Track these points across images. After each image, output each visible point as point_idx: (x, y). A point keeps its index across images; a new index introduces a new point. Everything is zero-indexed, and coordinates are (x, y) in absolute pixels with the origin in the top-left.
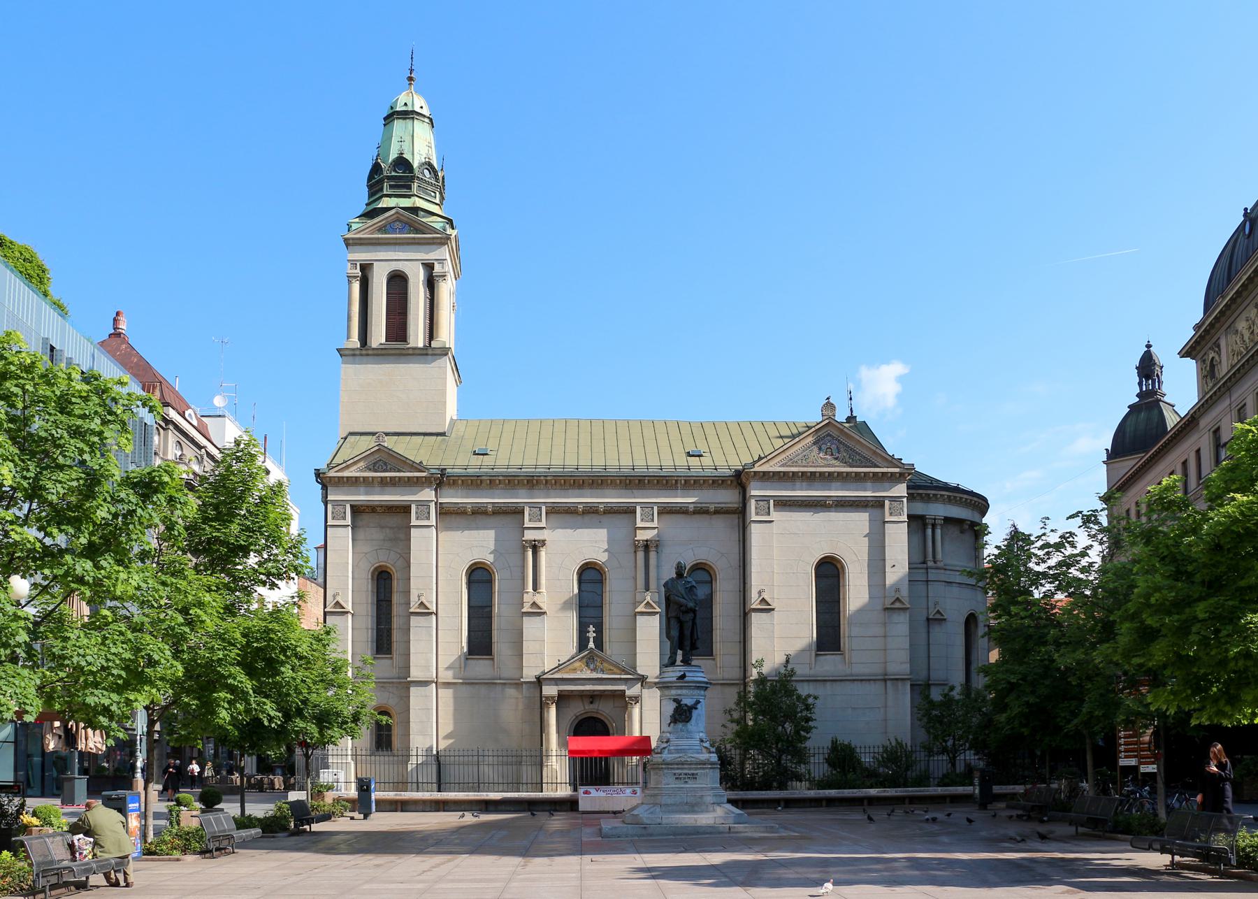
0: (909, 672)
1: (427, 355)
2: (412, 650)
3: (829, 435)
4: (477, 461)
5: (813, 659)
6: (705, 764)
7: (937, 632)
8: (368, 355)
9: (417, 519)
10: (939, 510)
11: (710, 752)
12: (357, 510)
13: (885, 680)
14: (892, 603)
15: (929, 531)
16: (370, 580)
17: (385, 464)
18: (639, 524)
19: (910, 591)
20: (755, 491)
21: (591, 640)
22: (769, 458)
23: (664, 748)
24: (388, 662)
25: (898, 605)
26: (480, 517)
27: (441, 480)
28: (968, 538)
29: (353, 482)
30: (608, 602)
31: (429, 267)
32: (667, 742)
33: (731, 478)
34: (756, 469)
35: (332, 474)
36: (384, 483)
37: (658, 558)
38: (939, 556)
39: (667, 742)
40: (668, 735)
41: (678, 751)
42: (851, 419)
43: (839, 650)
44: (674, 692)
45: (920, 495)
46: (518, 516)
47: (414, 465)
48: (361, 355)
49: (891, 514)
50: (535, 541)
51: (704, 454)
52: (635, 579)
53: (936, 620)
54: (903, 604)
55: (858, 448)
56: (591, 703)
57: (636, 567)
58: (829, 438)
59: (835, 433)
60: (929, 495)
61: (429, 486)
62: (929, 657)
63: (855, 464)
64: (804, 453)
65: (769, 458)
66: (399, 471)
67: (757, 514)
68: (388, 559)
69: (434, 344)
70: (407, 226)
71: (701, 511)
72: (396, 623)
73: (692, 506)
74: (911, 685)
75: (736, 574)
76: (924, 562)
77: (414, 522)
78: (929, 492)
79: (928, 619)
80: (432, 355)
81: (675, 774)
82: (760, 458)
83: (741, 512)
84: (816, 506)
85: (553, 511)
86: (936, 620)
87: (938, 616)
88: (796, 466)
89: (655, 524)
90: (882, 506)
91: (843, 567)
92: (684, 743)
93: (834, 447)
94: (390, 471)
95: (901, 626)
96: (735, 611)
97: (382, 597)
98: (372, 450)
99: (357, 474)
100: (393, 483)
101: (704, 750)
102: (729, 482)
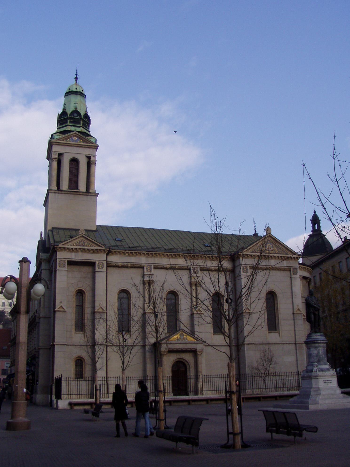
1: (88, 195)
8: (61, 193)
12: (71, 263)
17: (84, 242)
36: (84, 251)
48: (58, 193)
49: (294, 274)
63: (279, 253)
67: (243, 272)
93: (271, 246)
99: (72, 247)
100: (89, 251)
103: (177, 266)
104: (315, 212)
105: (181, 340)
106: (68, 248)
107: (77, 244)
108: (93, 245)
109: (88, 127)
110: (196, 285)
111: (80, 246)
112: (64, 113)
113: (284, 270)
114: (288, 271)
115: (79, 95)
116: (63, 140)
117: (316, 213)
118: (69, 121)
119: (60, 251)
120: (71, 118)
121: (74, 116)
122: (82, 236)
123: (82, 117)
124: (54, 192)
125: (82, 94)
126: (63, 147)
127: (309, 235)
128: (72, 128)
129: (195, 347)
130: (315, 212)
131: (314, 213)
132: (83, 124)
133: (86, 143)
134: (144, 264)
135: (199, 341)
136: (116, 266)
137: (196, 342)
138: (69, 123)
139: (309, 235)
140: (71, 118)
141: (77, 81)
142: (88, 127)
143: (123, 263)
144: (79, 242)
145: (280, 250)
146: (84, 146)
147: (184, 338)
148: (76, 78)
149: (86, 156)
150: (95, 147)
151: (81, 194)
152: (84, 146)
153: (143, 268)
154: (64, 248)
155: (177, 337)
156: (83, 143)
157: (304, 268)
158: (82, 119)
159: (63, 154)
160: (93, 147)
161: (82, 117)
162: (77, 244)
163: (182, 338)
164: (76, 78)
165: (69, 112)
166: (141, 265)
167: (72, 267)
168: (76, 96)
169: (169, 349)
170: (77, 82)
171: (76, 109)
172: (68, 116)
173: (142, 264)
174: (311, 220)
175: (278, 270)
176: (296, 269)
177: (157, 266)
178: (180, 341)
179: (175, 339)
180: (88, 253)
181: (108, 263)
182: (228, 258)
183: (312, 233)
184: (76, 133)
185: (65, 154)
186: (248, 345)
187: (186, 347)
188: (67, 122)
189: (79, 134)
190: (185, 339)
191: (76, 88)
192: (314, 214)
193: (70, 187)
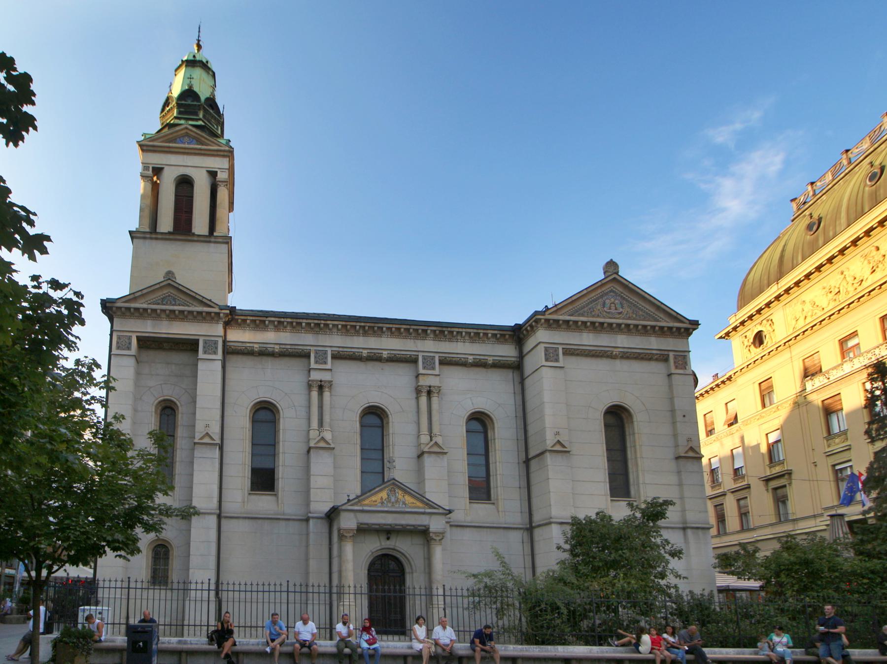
2: (195, 481)
9: (205, 352)
16: (153, 413)
17: (174, 299)
26: (265, 358)
33: (509, 333)
36: (173, 316)
46: (304, 360)
50: (321, 381)
52: (418, 424)
56: (388, 539)
68: (170, 392)
70: (195, 141)
71: (480, 364)
73: (471, 357)
77: (201, 354)
83: (517, 367)
85: (338, 356)
89: (437, 372)
98: (162, 284)
99: (145, 306)
105: (390, 505)
106: (137, 309)
108: (194, 304)
109: (215, 127)
110: (429, 393)
122: (169, 284)
129: (425, 523)
134: (308, 348)
135: (435, 508)
142: (215, 127)
143: (262, 345)
144: (162, 299)
146: (203, 152)
147: (397, 501)
149: (207, 171)
150: (226, 154)
152: (203, 152)
153: (307, 356)
154: (128, 309)
158: (201, 105)
160: (222, 153)
162: (160, 301)
163: (393, 499)
167: (151, 355)
169: (361, 524)
177: (339, 352)
178: (387, 506)
179: (376, 501)
180: (182, 320)
185: (166, 169)
187: (403, 522)
190: (401, 503)
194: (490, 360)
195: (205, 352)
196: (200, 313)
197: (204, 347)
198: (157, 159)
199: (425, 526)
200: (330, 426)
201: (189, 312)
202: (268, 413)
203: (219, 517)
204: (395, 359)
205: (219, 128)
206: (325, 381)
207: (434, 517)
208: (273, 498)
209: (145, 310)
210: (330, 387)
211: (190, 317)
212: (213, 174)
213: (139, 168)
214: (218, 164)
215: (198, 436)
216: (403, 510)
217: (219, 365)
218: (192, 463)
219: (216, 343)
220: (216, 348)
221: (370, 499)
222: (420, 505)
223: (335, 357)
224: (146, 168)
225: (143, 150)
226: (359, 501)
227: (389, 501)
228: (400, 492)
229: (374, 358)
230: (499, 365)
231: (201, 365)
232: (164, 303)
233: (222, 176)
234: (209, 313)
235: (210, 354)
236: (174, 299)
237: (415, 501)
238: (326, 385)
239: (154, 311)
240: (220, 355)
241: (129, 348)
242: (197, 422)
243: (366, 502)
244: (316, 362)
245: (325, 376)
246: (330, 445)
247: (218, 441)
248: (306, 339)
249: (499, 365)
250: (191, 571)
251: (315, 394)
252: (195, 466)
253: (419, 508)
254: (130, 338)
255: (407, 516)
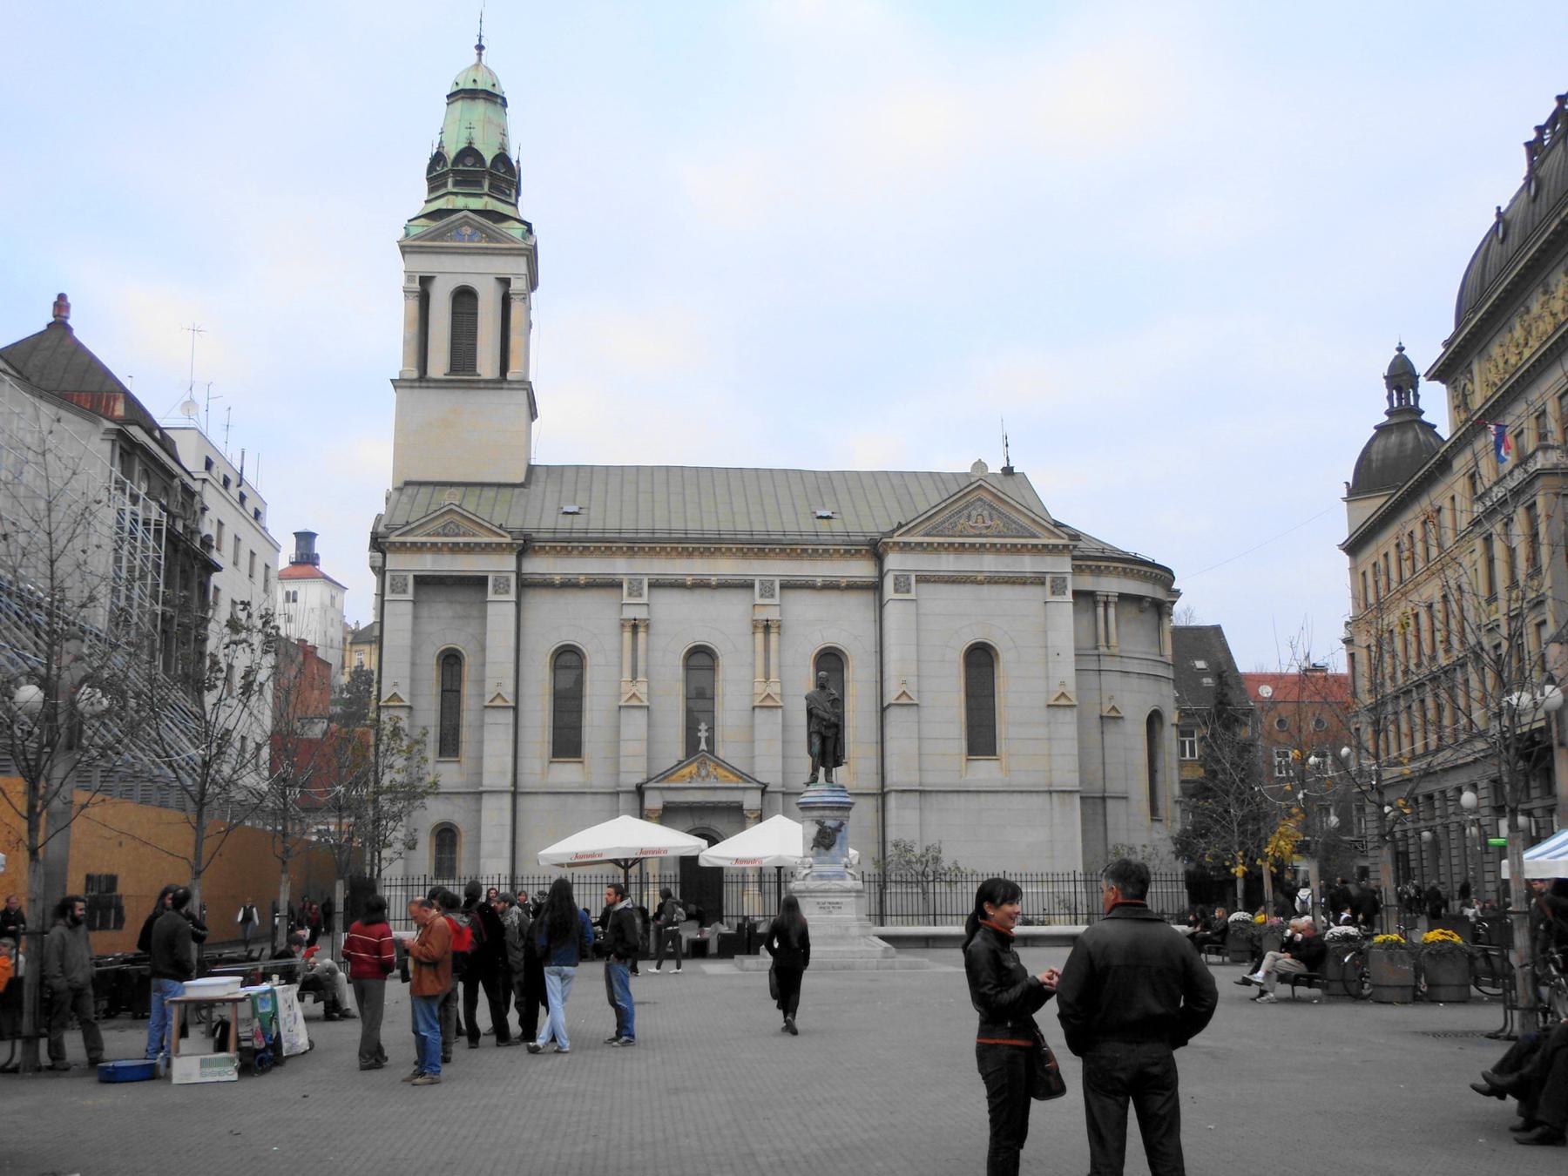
0: (1078, 783)
1: (502, 389)
3: (980, 499)
4: (565, 523)
5: (964, 764)
6: (850, 892)
7: (1113, 736)
8: (428, 387)
9: (496, 592)
10: (1111, 585)
11: (855, 879)
12: (424, 582)
13: (1050, 792)
14: (1057, 699)
15: (1101, 610)
17: (458, 526)
18: (759, 601)
19: (1079, 687)
20: (893, 561)
21: (703, 740)
22: (910, 525)
23: (807, 875)
24: (454, 766)
25: (1063, 702)
27: (525, 546)
28: (1150, 617)
29: (418, 548)
30: (720, 693)
31: (505, 282)
32: (810, 867)
34: (896, 539)
35: (393, 538)
36: (455, 549)
37: (780, 640)
38: (1113, 641)
39: (810, 867)
40: (811, 859)
41: (821, 877)
42: (1008, 471)
43: (995, 755)
44: (816, 813)
45: (1089, 567)
46: (618, 591)
47: (494, 528)
48: (420, 387)
49: (1053, 593)
51: (834, 516)
52: (753, 665)
53: (1110, 719)
54: (1070, 699)
55: (1014, 515)
57: (754, 652)
58: (979, 503)
59: (988, 498)
60: (1100, 567)
61: (511, 553)
62: (1104, 763)
64: (951, 521)
65: (910, 525)
66: (474, 535)
67: (896, 591)
68: (456, 638)
69: (510, 376)
71: (831, 586)
72: (468, 717)
74: (1081, 798)
75: (873, 660)
76: (1096, 648)
77: (491, 596)
78: (1100, 563)
79: (1102, 717)
80: (509, 389)
81: (818, 903)
82: (900, 526)
83: (876, 587)
84: (965, 582)
86: (1110, 719)
87: (1113, 714)
88: (941, 536)
90: (1043, 583)
91: (997, 655)
92: (826, 869)
93: (985, 513)
94: (464, 535)
95: (1067, 725)
96: (871, 706)
97: (448, 687)
99: (424, 539)
100: (469, 549)
101: (849, 877)
102: (864, 552)
103: (713, 578)
104: (1401, 349)
105: (699, 780)
106: (414, 544)
107: (440, 530)
111: (446, 535)
112: (438, 158)
113: (1024, 583)
114: (1036, 584)
115: (481, 101)
116: (433, 239)
117: (1404, 352)
118: (450, 181)
119: (391, 551)
120: (456, 173)
121: (465, 165)
122: (451, 510)
123: (488, 162)
124: (408, 384)
125: (494, 98)
126: (433, 258)
127: (1376, 427)
128: (460, 202)
130: (1401, 349)
131: (1397, 353)
132: (491, 186)
133: (498, 242)
136: (546, 584)
137: (742, 785)
138: (450, 188)
139: (1376, 427)
140: (456, 173)
141: (480, 55)
145: (1014, 526)
148: (480, 48)
151: (482, 385)
153: (620, 585)
154: (404, 544)
155: (691, 772)
156: (490, 241)
157: (1124, 569)
159: (434, 277)
161: (488, 162)
163: (703, 773)
164: (480, 48)
165: (451, 152)
166: (614, 580)
168: (473, 103)
169: (668, 803)
170: (483, 57)
171: (470, 143)
172: (449, 162)
173: (618, 577)
174: (1385, 377)
175: (1006, 583)
176: (1064, 580)
181: (524, 577)
182: (864, 552)
183: (1386, 418)
184: (465, 216)
185: (439, 277)
186: (900, 794)
188: (445, 185)
189: (477, 218)
191: (475, 81)
192: (1396, 357)
193: (454, 368)
194: (844, 582)
195: (496, 592)
196: (488, 545)
197: (494, 586)
198: (426, 264)
199: (738, 802)
200: (647, 675)
201: (476, 544)
202: (575, 658)
203: (515, 794)
204: (726, 585)
205: (514, 191)
206: (640, 620)
207: (748, 792)
208: (579, 766)
209: (424, 544)
210: (647, 626)
211: (477, 549)
212: (505, 282)
213: (401, 280)
214: (515, 267)
215: (488, 697)
216: (712, 785)
217: (512, 607)
218: (482, 726)
219: (508, 579)
220: (509, 586)
221: (677, 775)
222: (735, 779)
223: (652, 586)
224: (410, 278)
225: (404, 253)
226: (665, 778)
227: (700, 776)
228: (712, 764)
229: (701, 585)
230: (853, 587)
231: (491, 609)
232: (446, 531)
233: (517, 285)
234: (499, 544)
235: (501, 593)
236: (458, 526)
237: (728, 774)
238: (642, 624)
239: (434, 544)
240: (512, 596)
241: (405, 591)
242: (487, 680)
243: (674, 777)
244: (630, 595)
245: (641, 613)
246: (642, 701)
247: (512, 704)
248: (619, 566)
249: (853, 587)
250: (482, 861)
251: (627, 635)
252: (487, 736)
253: (731, 781)
254: (405, 578)
255: (718, 792)
